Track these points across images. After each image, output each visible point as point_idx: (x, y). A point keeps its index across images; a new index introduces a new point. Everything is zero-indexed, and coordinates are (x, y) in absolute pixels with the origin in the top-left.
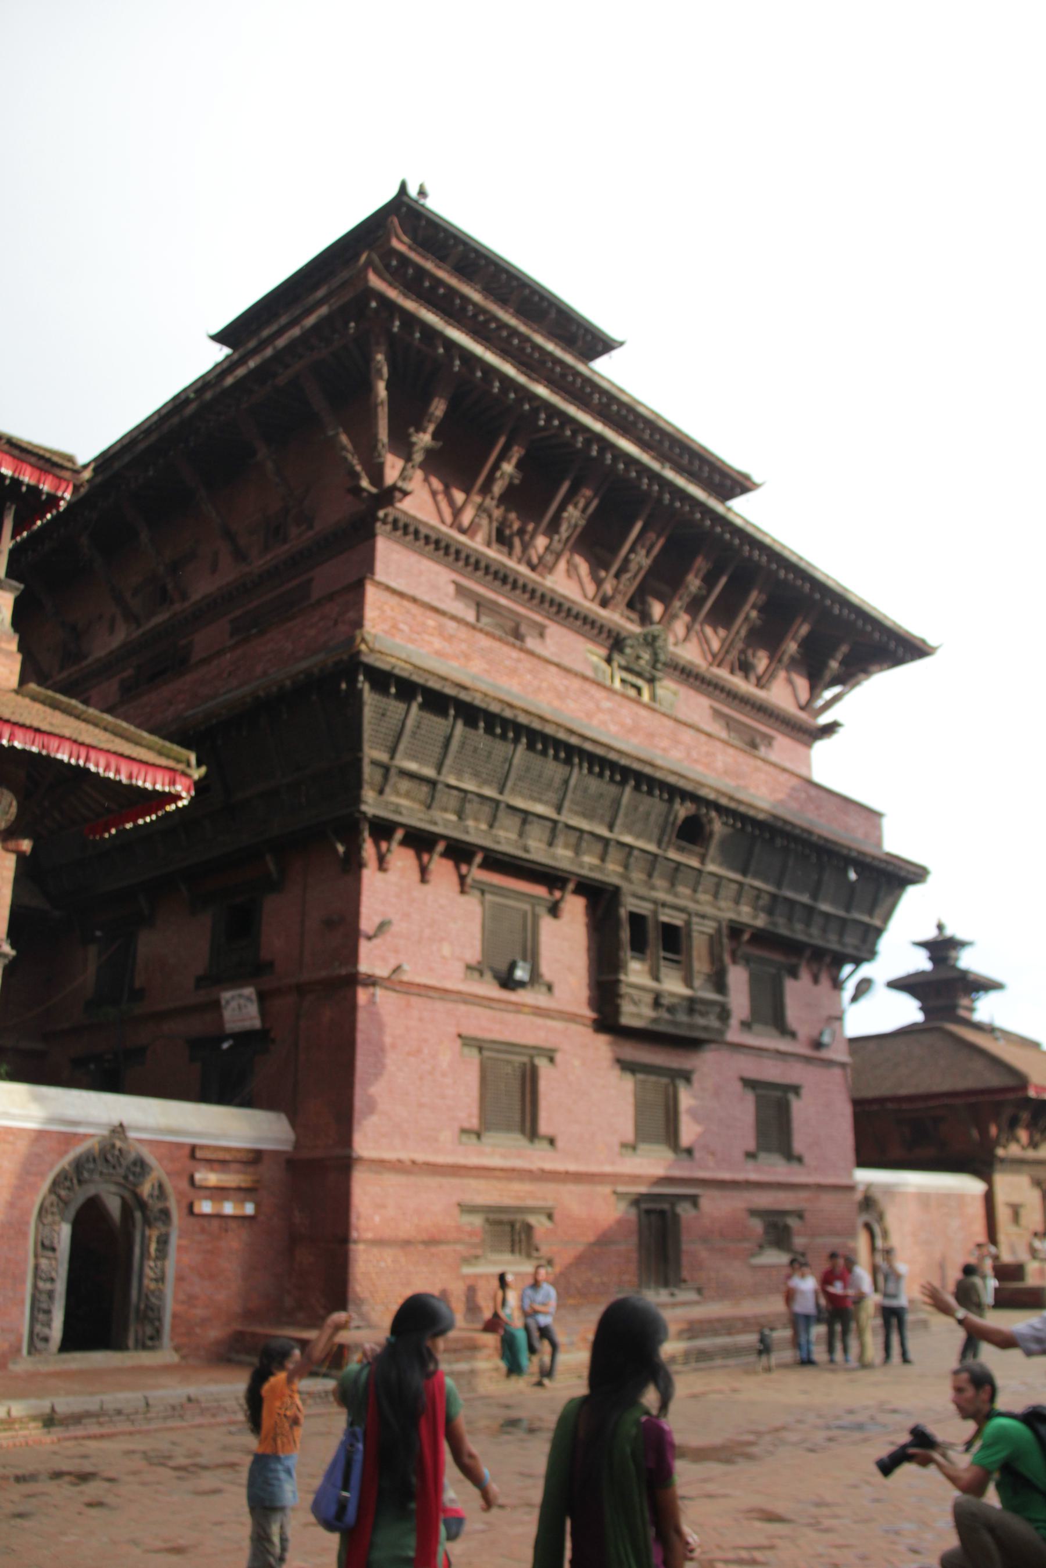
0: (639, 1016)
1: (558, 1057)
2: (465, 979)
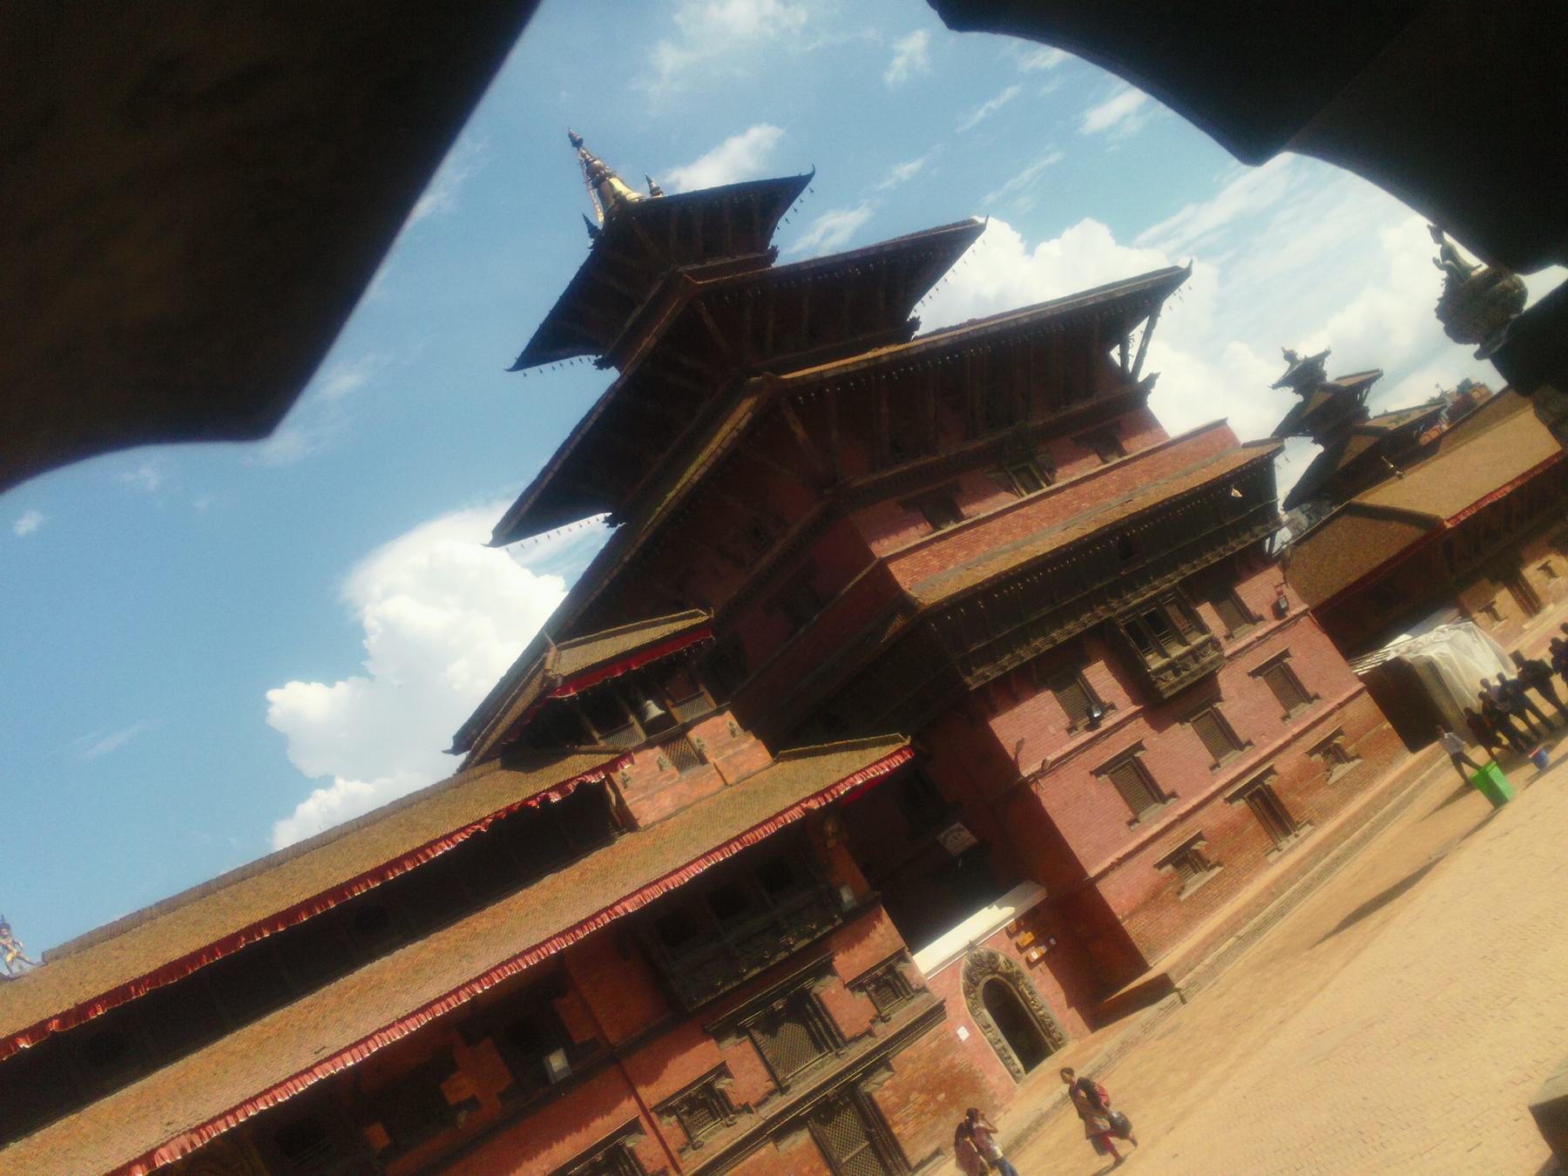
0: (1173, 686)
1: (1145, 743)
2: (1072, 739)
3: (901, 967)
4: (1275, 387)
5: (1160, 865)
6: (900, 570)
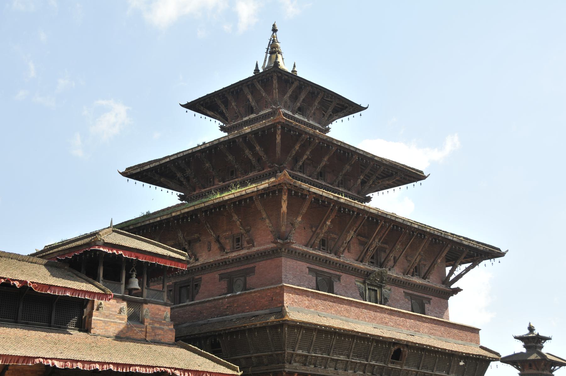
4: (516, 338)
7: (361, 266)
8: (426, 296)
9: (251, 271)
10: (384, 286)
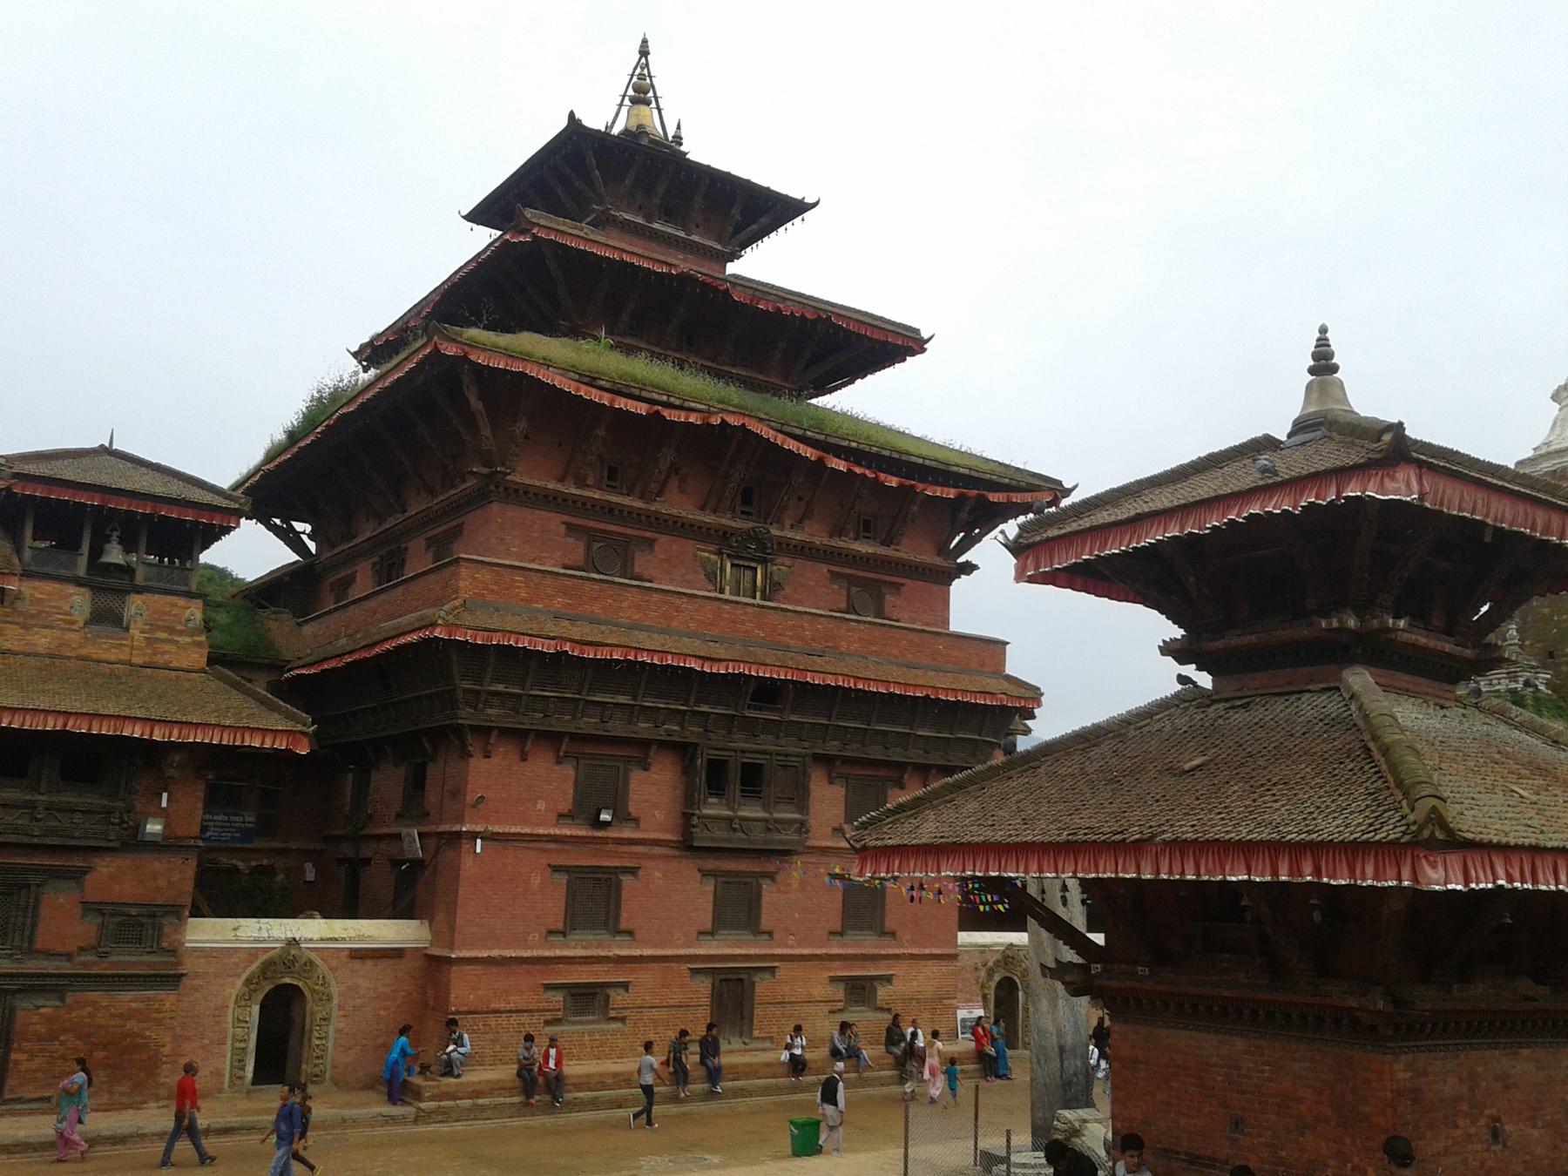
0: (713, 840)
1: (640, 873)
2: (557, 825)
3: (168, 923)
5: (548, 987)
6: (473, 577)
7: (708, 518)
8: (888, 578)
9: (456, 532)
10: (772, 561)
